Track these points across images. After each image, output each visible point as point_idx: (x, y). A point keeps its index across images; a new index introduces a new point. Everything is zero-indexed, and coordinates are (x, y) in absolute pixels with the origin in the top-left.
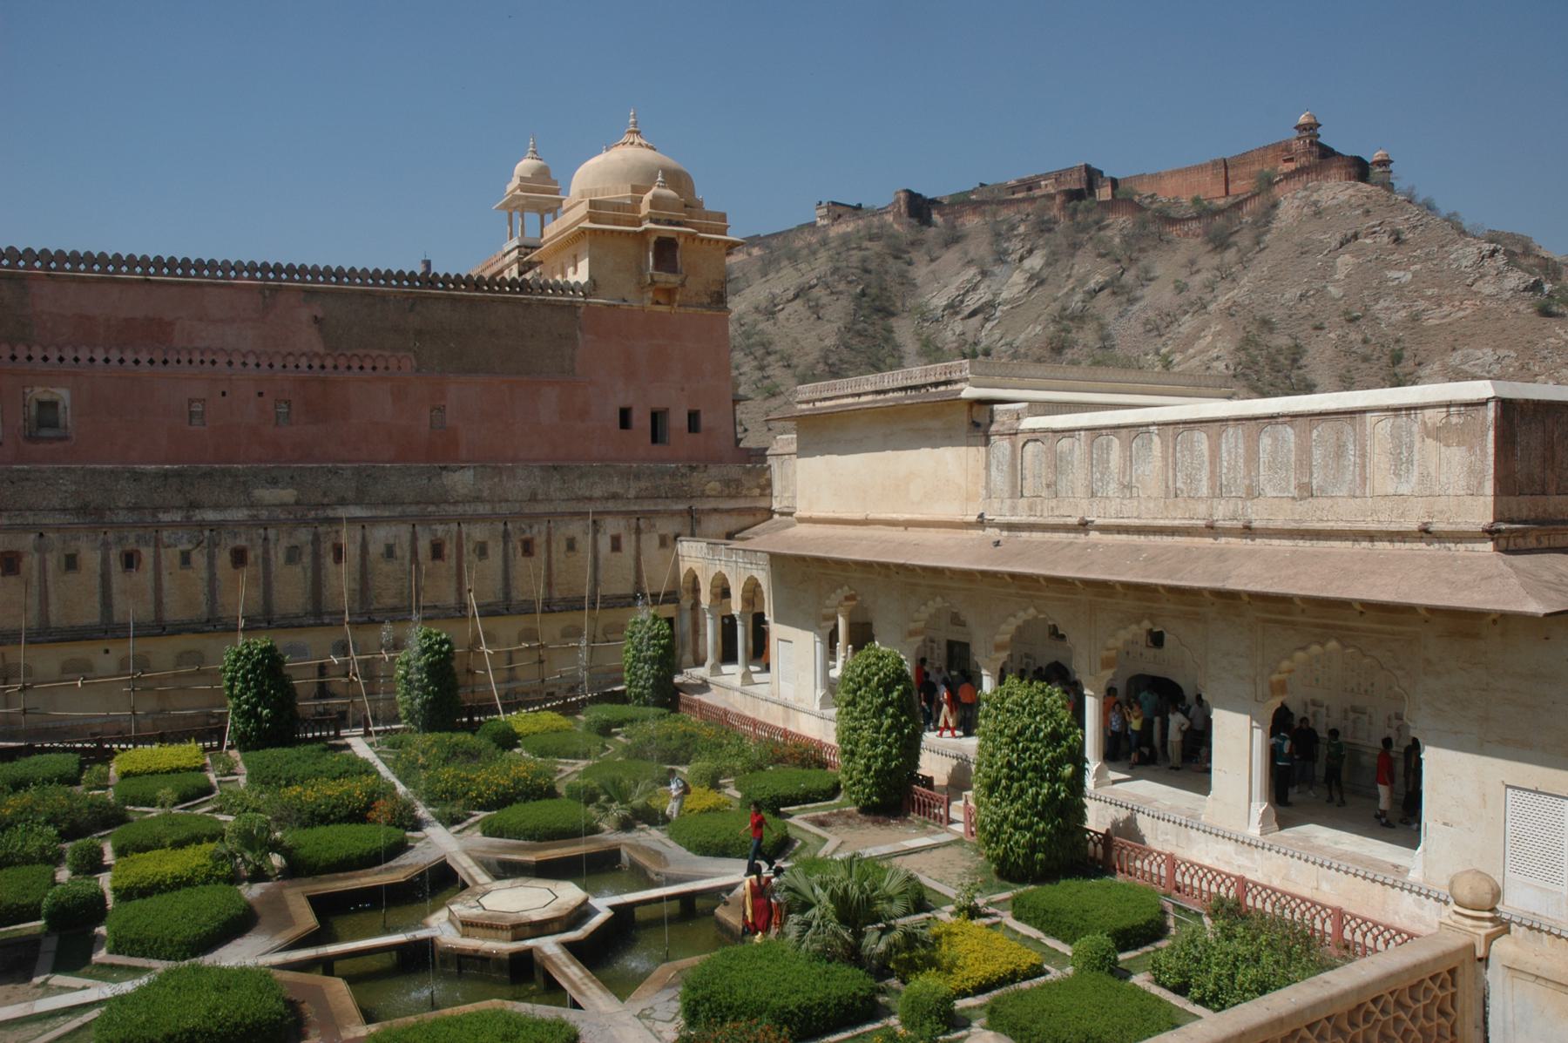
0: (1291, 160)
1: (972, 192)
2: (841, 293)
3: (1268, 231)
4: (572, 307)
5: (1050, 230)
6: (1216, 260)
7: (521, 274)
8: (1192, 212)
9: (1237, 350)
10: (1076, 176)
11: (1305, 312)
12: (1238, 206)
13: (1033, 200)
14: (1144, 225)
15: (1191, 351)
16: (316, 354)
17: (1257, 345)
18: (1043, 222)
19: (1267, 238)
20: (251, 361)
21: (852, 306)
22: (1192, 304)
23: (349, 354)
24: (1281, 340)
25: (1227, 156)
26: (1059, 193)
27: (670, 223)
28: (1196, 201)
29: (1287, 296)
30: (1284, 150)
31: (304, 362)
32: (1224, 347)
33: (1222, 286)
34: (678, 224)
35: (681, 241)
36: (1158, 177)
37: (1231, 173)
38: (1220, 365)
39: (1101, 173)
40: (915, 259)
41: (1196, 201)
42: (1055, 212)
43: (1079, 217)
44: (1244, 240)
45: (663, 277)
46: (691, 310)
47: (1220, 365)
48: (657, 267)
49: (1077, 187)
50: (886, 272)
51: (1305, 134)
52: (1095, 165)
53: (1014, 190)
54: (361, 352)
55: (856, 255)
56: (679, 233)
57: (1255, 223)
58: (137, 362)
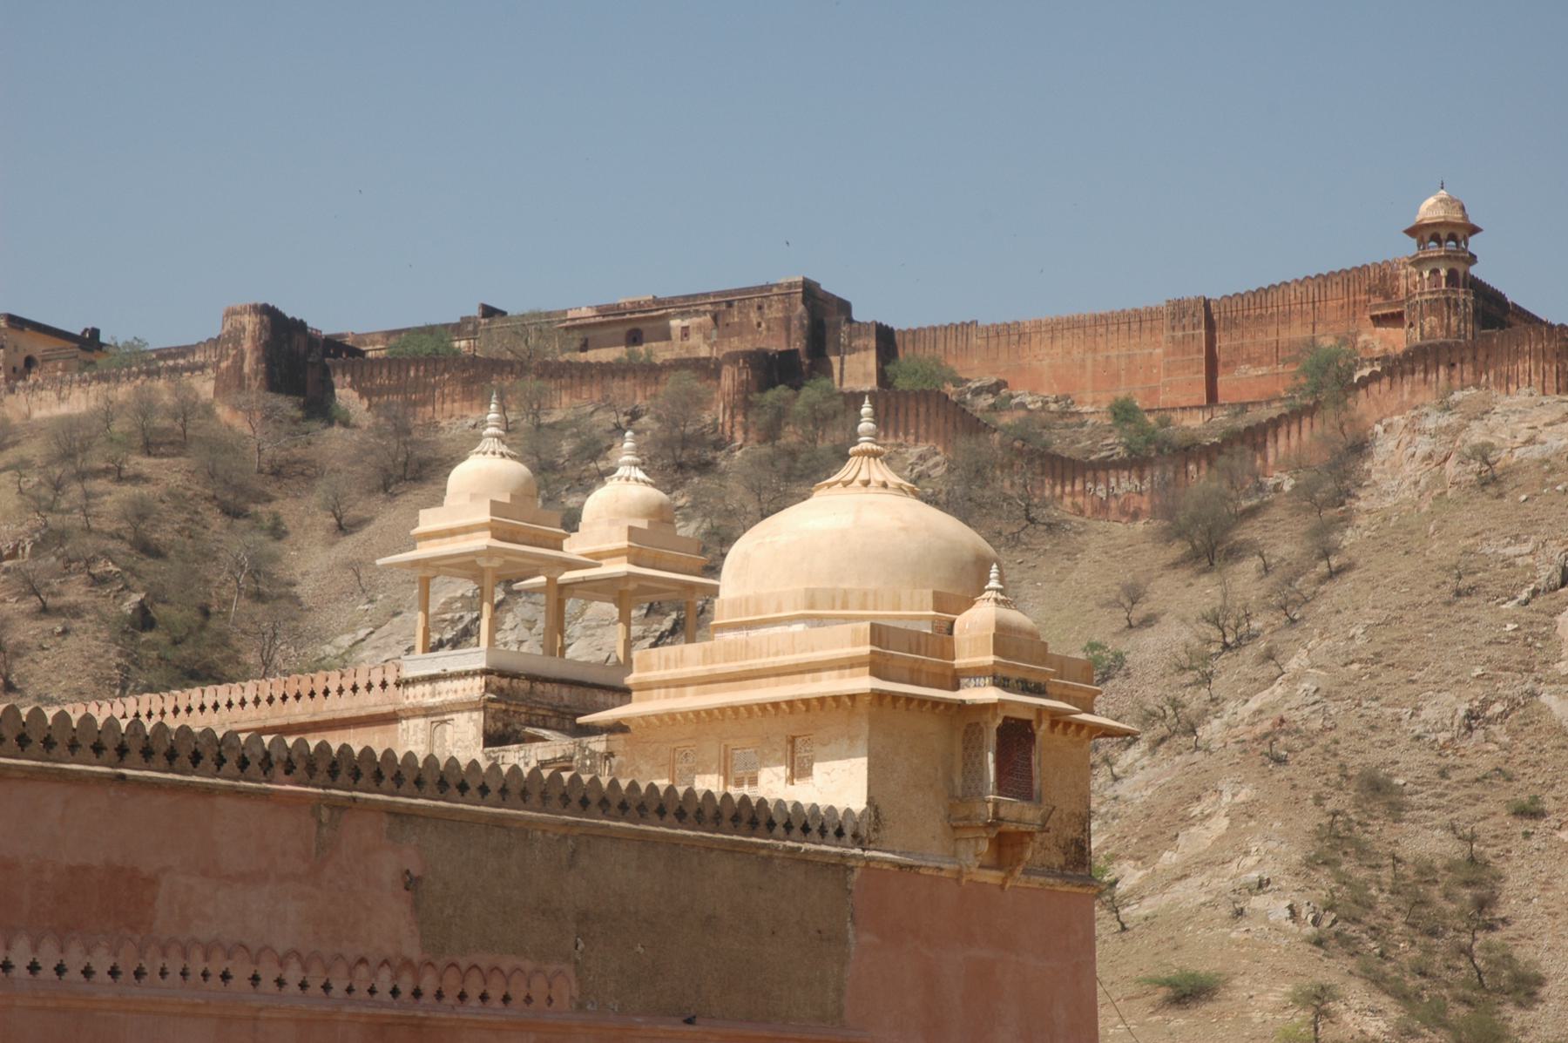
0: (1395, 319)
1: (458, 329)
2: (75, 612)
3: (1346, 520)
4: (840, 866)
5: (705, 467)
6: (1205, 592)
7: (493, 739)
8: (1114, 444)
9: (1311, 863)
10: (775, 312)
11: (1484, 764)
12: (1255, 437)
13: (652, 371)
14: (978, 473)
15: (1169, 858)
16: (407, 963)
17: (1362, 851)
18: (685, 442)
19: (1348, 538)
20: (293, 974)
21: (114, 657)
22: (1149, 718)
23: (464, 963)
24: (1427, 842)
25: (1214, 294)
26: (733, 358)
27: (1027, 688)
28: (1123, 412)
29: (1428, 713)
30: (1376, 291)
31: (384, 981)
32: (1271, 851)
33: (1232, 671)
34: (1039, 690)
35: (1042, 730)
36: (1012, 335)
37: (1223, 343)
38: (1274, 907)
39: (845, 307)
40: (289, 522)
41: (1123, 412)
42: (717, 413)
43: (791, 436)
44: (1282, 539)
45: (1019, 812)
46: (1036, 881)
47: (1274, 907)
48: (1001, 788)
49: (777, 345)
50: (208, 556)
51: (1433, 249)
52: (829, 285)
53: (586, 334)
54: (485, 960)
55: (113, 498)
56: (1040, 710)
57: (1305, 492)
58: (87, 972)
